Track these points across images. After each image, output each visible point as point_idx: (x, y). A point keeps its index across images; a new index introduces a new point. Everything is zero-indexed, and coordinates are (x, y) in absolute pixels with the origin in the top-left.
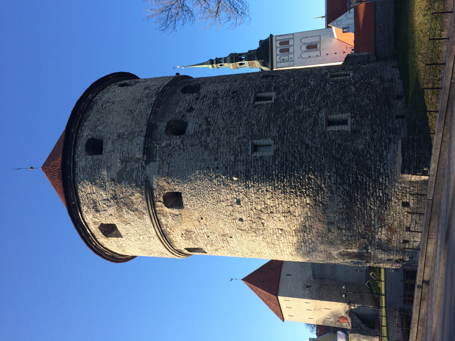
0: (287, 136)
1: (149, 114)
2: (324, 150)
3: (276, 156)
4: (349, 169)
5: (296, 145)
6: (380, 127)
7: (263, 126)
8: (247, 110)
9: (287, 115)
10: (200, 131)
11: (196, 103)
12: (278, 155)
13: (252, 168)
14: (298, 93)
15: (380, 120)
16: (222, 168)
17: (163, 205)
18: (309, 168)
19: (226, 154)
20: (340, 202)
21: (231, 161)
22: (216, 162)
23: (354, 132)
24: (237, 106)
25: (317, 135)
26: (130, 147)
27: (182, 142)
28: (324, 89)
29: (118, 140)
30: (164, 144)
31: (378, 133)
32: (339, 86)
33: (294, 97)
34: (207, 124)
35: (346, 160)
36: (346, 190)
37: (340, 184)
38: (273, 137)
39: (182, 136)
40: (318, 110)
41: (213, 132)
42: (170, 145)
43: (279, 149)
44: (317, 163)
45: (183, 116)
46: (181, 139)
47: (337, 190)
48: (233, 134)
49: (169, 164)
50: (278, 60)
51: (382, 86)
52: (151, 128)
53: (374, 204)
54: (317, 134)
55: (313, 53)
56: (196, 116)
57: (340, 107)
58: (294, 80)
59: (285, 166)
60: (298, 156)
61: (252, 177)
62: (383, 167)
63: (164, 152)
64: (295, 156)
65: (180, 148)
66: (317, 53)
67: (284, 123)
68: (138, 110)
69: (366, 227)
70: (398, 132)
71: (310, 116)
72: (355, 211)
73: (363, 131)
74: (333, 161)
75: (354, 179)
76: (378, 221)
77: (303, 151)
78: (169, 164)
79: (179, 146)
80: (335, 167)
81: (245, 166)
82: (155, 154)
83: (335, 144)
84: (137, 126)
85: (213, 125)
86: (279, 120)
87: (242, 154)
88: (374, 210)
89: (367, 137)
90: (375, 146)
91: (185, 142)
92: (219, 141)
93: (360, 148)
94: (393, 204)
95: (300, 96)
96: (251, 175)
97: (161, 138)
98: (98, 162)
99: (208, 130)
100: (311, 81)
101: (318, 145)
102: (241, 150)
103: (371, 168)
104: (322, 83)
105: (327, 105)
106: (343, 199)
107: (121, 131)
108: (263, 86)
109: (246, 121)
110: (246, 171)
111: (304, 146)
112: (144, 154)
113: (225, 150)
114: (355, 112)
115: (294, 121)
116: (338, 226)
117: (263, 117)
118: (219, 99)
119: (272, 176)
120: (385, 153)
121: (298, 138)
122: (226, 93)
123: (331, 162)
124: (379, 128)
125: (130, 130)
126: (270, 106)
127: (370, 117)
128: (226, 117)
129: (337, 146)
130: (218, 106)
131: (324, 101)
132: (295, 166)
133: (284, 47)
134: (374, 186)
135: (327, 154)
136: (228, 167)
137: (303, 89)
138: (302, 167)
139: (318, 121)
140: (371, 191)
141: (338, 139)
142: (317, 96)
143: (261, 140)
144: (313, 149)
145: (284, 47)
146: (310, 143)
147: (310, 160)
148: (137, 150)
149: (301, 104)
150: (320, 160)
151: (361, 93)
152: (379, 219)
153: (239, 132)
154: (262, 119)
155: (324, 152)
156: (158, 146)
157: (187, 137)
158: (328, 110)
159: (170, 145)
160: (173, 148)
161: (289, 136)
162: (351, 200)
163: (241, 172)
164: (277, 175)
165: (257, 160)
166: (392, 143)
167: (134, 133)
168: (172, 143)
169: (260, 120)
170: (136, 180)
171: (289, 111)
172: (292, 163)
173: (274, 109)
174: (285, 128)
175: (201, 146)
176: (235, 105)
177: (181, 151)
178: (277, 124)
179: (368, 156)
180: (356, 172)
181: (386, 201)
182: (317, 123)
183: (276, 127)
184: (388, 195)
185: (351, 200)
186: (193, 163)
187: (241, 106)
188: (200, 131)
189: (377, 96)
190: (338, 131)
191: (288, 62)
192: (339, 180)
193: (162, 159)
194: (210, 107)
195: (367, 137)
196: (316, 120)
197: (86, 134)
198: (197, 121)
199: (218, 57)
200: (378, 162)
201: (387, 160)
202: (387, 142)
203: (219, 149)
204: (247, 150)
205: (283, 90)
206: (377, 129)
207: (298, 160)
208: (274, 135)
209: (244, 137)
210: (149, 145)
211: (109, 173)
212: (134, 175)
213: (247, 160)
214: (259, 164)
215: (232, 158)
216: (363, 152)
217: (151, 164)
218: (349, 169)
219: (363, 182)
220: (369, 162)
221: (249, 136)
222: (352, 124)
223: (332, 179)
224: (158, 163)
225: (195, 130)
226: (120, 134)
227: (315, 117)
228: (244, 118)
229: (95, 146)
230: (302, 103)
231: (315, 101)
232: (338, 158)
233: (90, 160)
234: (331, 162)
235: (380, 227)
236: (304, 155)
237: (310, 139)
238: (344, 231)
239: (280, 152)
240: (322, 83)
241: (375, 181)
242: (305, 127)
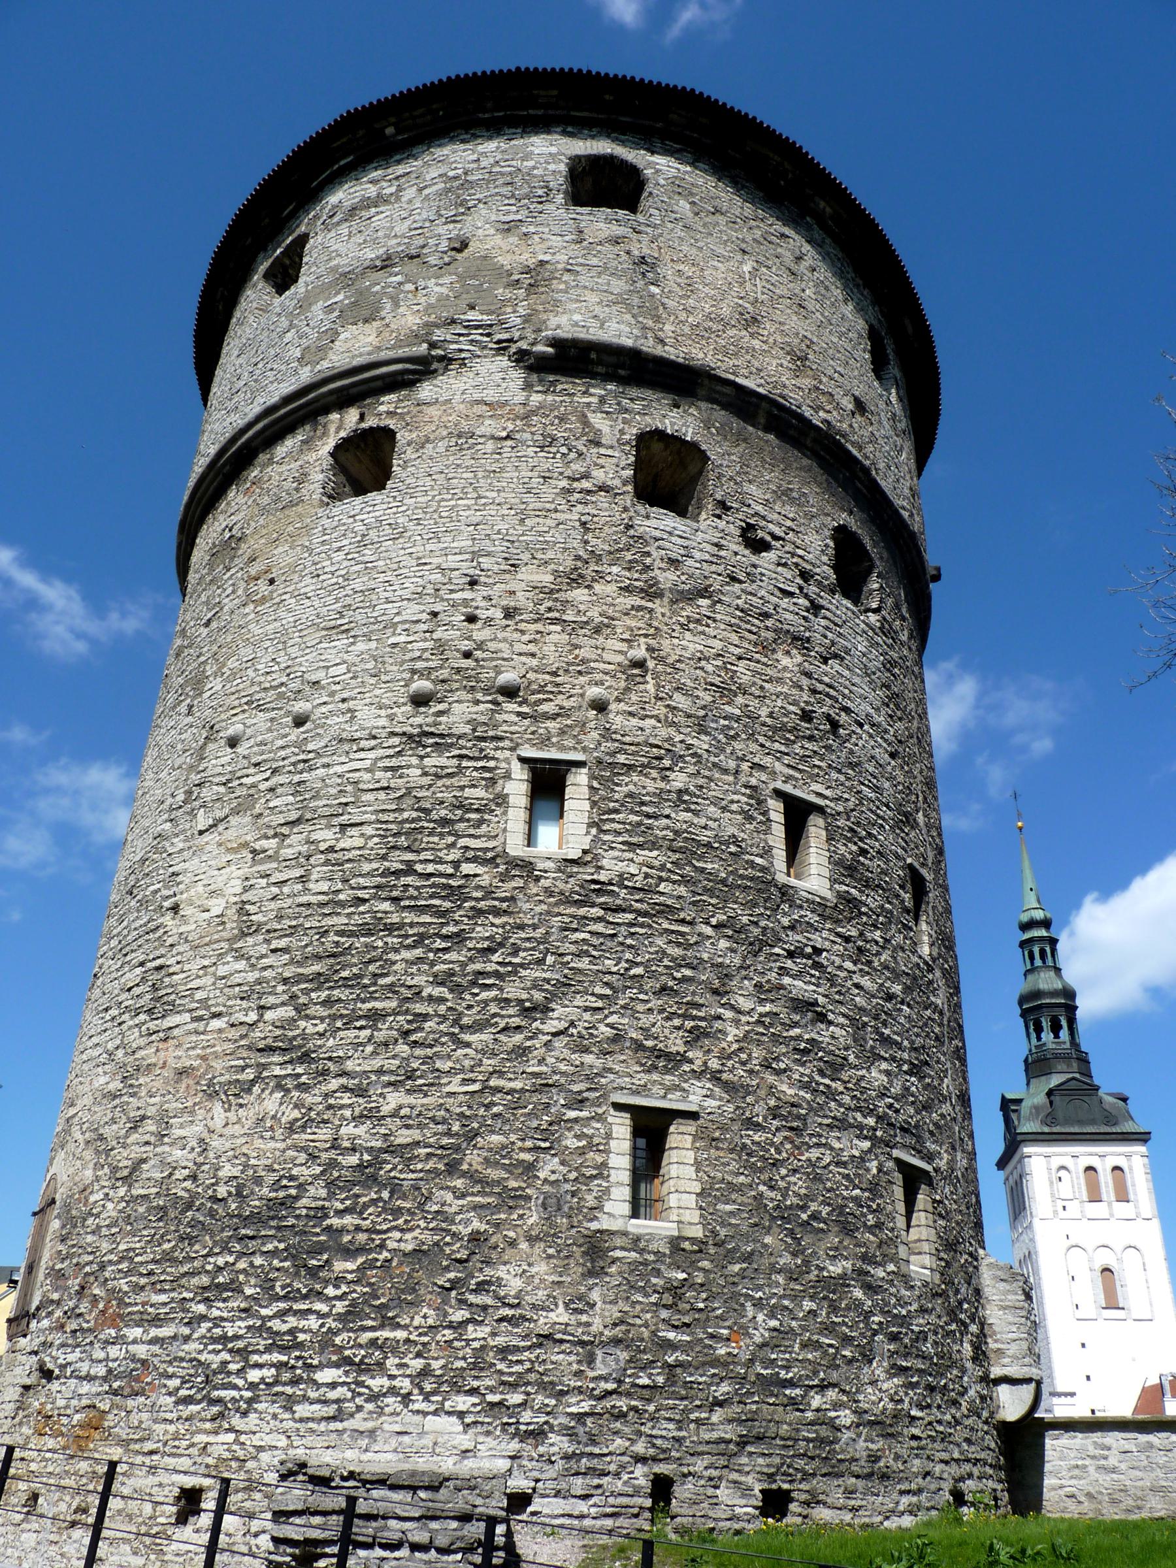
0: (600, 919)
1: (739, 380)
2: (511, 1092)
3: (502, 868)
4: (396, 1213)
5: (550, 959)
6: (611, 1386)
7: (655, 817)
8: (742, 760)
9: (708, 931)
10: (648, 561)
11: (785, 565)
12: (505, 877)
13: (455, 762)
14: (821, 1000)
15: (653, 1387)
16: (469, 638)
17: (343, 434)
18: (425, 1017)
19: (533, 655)
20: (246, 1166)
21: (499, 673)
22: (499, 614)
23: (596, 1249)
24: (764, 724)
25: (589, 1059)
26: (593, 298)
27: (603, 488)
28: (841, 1124)
29: (624, 257)
31: (579, 1374)
32: (855, 1199)
33: (798, 976)
34: (682, 592)
35: (449, 1197)
36: (296, 1198)
37: (332, 1164)
38: (596, 857)
39: (630, 488)
40: (725, 1076)
41: (640, 608)
43: (537, 879)
44: (449, 1057)
45: (723, 505)
46: (617, 482)
47: (303, 1149)
48: (627, 689)
49: (508, 437)
50: (1056, 1162)
51: (846, 1417)
52: (681, 381)
53: (215, 1340)
54: (598, 1063)
55: (1089, 1292)
56: (722, 553)
57: (739, 1189)
58: (890, 997)
59: (447, 904)
60: (491, 967)
61: (414, 761)
62: (393, 1391)
63: (562, 419)
64: (490, 950)
65: (578, 480)
66: (1089, 1308)
67: (666, 910)
68: (756, 343)
69: (121, 1303)
70: (579, 1485)
71: (696, 1036)
72: (191, 1240)
73: (595, 1296)
74: (449, 1134)
75: (347, 1238)
76: (134, 1358)
77: (513, 990)
78: (508, 437)
79: (586, 476)
80: (417, 1144)
81: (467, 729)
82: (559, 387)
83: (536, 1149)
84: (687, 330)
85: (674, 613)
86: (682, 890)
87: (527, 722)
88: (187, 1339)
89: (560, 1315)
90: (504, 1352)
92: (597, 630)
93: (501, 1272)
94: (201, 1438)
95: (803, 1005)
96: (422, 758)
97: (626, 411)
98: (540, 192)
99: (651, 592)
100: (888, 1073)
101: (542, 1061)
102: (547, 716)
103: (398, 1326)
104: (871, 1121)
105: (750, 1124)
106: (258, 1181)
107: (667, 271)
108: (863, 852)
109: (689, 747)
110: (442, 736)
111: (538, 996)
112: (556, 343)
113: (549, 649)
114: (705, 1264)
115: (673, 960)
116: (144, 1161)
117: (703, 821)
118: (799, 659)
119: (408, 849)
120: (463, 1402)
121: (580, 971)
122: (832, 692)
123: (444, 1121)
124: (605, 1378)
125: (670, 303)
126: (759, 860)
127: (671, 1335)
128: (710, 668)
129: (524, 1156)
130: (766, 648)
131: (774, 1113)
132: (445, 950)
133: (1106, 1179)
134: (301, 1337)
135: (488, 1107)
136: (469, 663)
137: (842, 1026)
138: (439, 980)
139: (667, 1071)
140: (276, 1325)
141: (562, 1163)
142: (805, 1086)
143: (587, 805)
144: (518, 1038)
145: (1106, 1179)
146: (552, 1025)
147: (465, 1021)
148: (577, 317)
149: (761, 1002)
150: (462, 1071)
151: (808, 1305)
152: (144, 1362)
153: (631, 714)
154: (688, 816)
155: (498, 1090)
156: (594, 400)
157: (626, 509)
158: (723, 1128)
160: (580, 454)
161: (599, 927)
162: (246, 1220)
163: (441, 713)
164: (409, 870)
165: (492, 781)
166: (515, 1445)
167: (657, 319)
168: (603, 451)
169: (688, 810)
170: (453, 322)
171: (723, 944)
172: (459, 939)
173: (742, 877)
174: (639, 913)
175: (578, 558)
176: (771, 715)
177: (564, 483)
178: (661, 879)
179: (459, 1315)
180: (382, 1246)
181: (219, 1401)
182: (655, 1067)
183: (647, 876)
184: (245, 1414)
185: (246, 1220)
186: (503, 526)
187: (762, 739)
188: (648, 561)
189: (791, 1383)
190: (604, 1165)
191: (1052, 1195)
192: (354, 1160)
193: (534, 413)
194: (767, 615)
195: (560, 1315)
196: (674, 1061)
198: (698, 555)
199: (1059, 946)
200: (418, 1364)
201: (425, 1414)
202: (526, 1416)
203: (558, 628)
204: (545, 742)
205: (838, 935)
206: (601, 1370)
207: (471, 967)
208: (605, 862)
209: (607, 734)
210: (600, 369)
211: (492, 231)
213: (501, 739)
214: (468, 792)
215: (508, 677)
216: (481, 1287)
217: (517, 376)
218: (396, 1213)
219: (327, 1282)
220: (426, 1315)
221: (613, 754)
222: (636, 1242)
223: (361, 1130)
224: (520, 397)
225: (657, 539)
226: (653, 266)
227: (691, 1061)
228: (702, 744)
229: (604, 187)
230: (768, 1008)
231: (778, 1072)
232: (459, 1162)
233: (552, 167)
234: (444, 1121)
235: (110, 1371)
236: (493, 993)
237: (572, 1024)
238: (122, 1191)
239: (519, 883)
240: (871, 1121)
241: (325, 1342)
242: (640, 1007)
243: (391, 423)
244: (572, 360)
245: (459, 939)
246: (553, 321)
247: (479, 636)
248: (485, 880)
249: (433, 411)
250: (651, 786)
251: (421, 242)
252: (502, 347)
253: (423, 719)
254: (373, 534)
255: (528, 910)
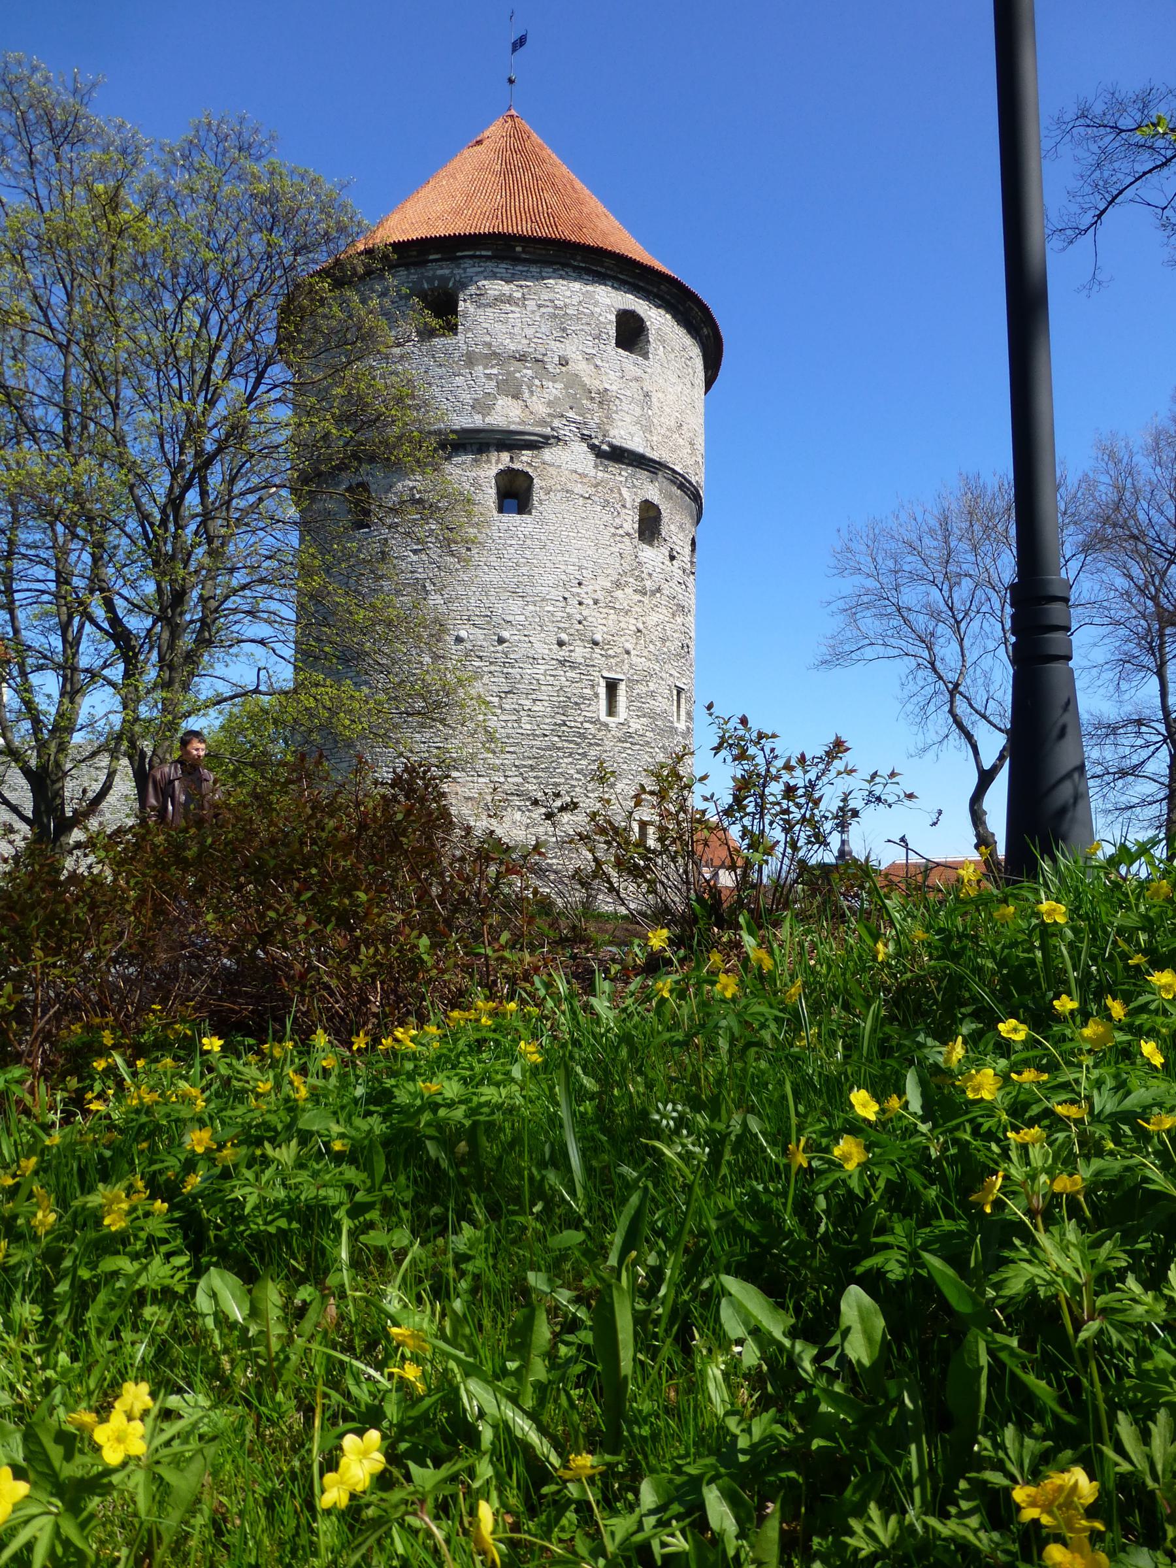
1: (677, 468)
12: (599, 730)
17: (501, 467)
26: (628, 419)
27: (628, 534)
30: (624, 491)
42: (624, 506)
91: (626, 539)
159: (624, 506)
172: (584, 755)
197: (657, 319)
204: (610, 669)
212: (571, 414)
217: (591, 457)
229: (630, 333)
243: (530, 470)
244: (618, 455)
245: (584, 755)
246: (612, 433)
247: (585, 613)
248: (593, 731)
249: (552, 470)
250: (645, 689)
251: (543, 351)
252: (585, 438)
253: (563, 653)
254: (528, 542)
255: (608, 744)
